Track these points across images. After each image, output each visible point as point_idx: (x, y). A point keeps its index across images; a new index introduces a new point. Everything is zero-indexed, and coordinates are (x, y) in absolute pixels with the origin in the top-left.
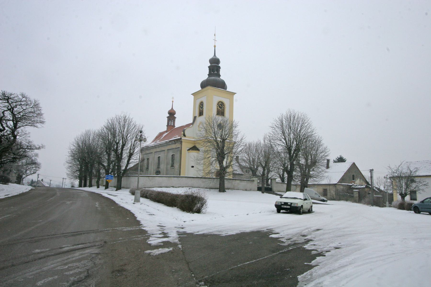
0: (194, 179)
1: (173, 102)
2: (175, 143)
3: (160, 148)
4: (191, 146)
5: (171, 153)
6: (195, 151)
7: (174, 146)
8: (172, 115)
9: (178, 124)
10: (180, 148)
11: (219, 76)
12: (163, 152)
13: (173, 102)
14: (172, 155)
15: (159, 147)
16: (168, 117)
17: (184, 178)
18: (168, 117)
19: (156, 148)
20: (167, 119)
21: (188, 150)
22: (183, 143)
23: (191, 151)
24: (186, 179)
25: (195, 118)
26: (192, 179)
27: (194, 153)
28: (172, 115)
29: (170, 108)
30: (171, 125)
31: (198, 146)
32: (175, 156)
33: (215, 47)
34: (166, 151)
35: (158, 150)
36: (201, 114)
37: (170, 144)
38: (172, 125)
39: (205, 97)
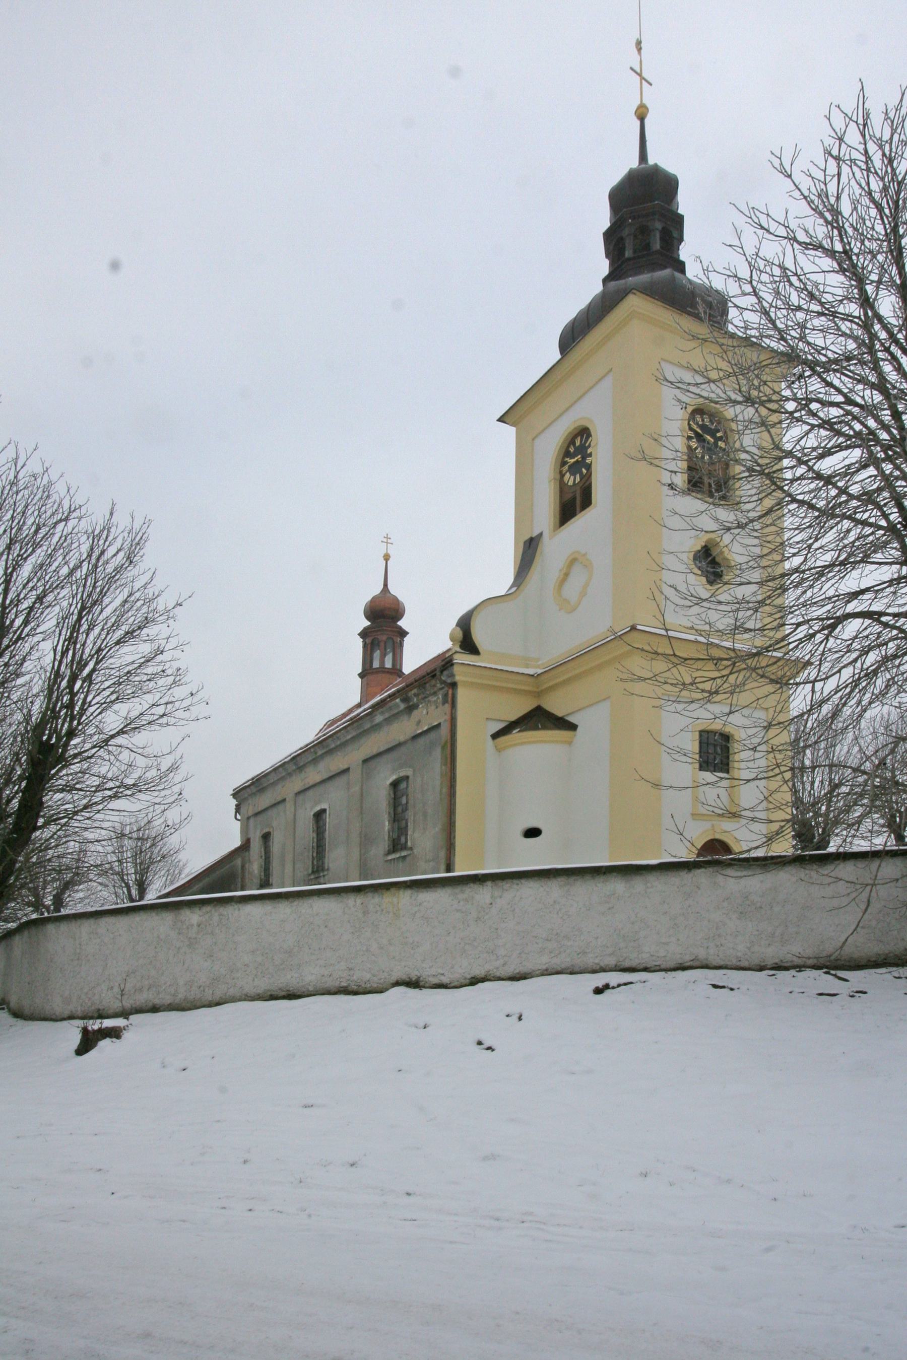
0: (638, 883)
1: (387, 558)
2: (411, 709)
3: (322, 765)
4: (519, 708)
5: (385, 776)
6: (545, 728)
7: (402, 729)
8: (383, 622)
9: (415, 656)
10: (445, 731)
11: (681, 267)
12: (343, 779)
13: (387, 558)
14: (395, 785)
15: (315, 761)
16: (364, 634)
17: (529, 890)
18: (364, 634)
19: (300, 769)
20: (360, 641)
21: (495, 736)
22: (462, 694)
23: (516, 735)
24: (554, 888)
25: (529, 550)
26: (617, 885)
27: (536, 750)
28: (383, 622)
29: (377, 589)
30: (382, 670)
31: (556, 705)
32: (415, 785)
33: (641, 115)
34: (355, 775)
35: (313, 775)
36: (573, 503)
37: (377, 727)
38: (388, 664)
39: (607, 383)
